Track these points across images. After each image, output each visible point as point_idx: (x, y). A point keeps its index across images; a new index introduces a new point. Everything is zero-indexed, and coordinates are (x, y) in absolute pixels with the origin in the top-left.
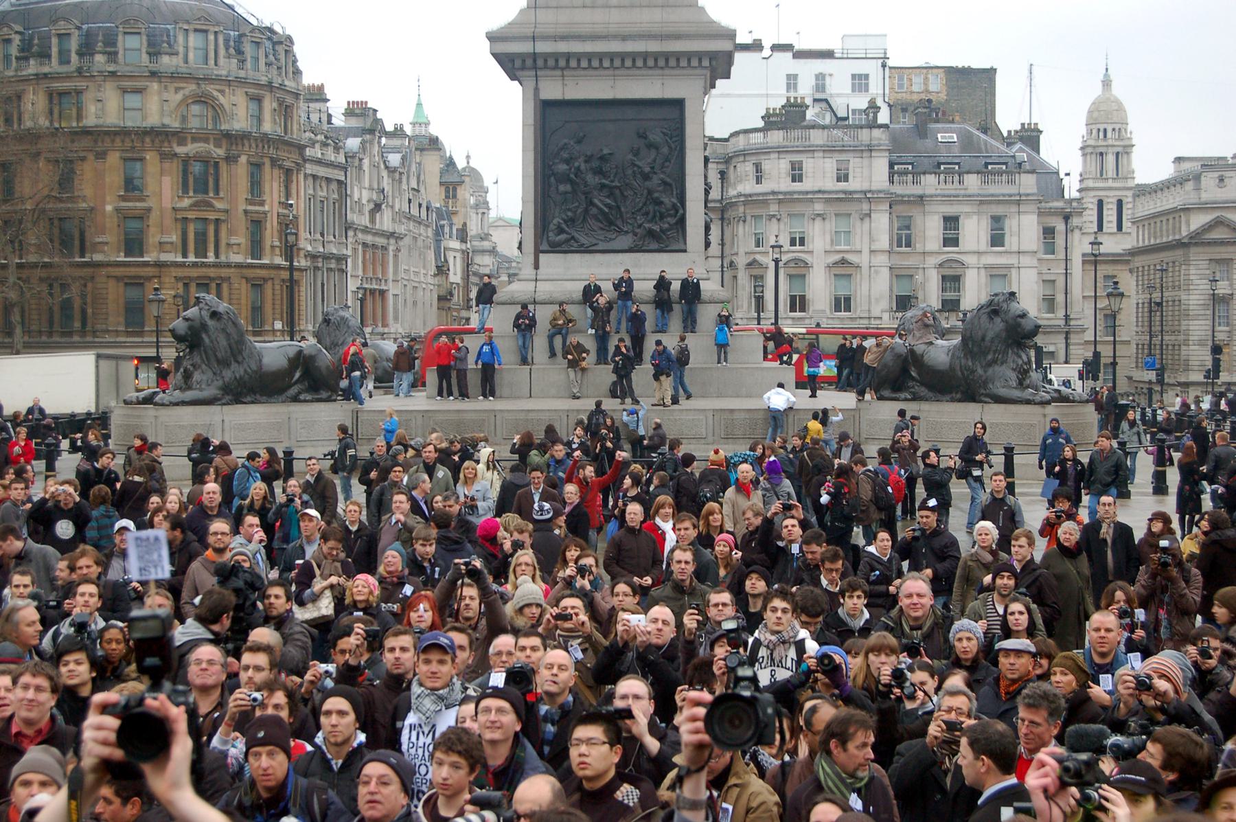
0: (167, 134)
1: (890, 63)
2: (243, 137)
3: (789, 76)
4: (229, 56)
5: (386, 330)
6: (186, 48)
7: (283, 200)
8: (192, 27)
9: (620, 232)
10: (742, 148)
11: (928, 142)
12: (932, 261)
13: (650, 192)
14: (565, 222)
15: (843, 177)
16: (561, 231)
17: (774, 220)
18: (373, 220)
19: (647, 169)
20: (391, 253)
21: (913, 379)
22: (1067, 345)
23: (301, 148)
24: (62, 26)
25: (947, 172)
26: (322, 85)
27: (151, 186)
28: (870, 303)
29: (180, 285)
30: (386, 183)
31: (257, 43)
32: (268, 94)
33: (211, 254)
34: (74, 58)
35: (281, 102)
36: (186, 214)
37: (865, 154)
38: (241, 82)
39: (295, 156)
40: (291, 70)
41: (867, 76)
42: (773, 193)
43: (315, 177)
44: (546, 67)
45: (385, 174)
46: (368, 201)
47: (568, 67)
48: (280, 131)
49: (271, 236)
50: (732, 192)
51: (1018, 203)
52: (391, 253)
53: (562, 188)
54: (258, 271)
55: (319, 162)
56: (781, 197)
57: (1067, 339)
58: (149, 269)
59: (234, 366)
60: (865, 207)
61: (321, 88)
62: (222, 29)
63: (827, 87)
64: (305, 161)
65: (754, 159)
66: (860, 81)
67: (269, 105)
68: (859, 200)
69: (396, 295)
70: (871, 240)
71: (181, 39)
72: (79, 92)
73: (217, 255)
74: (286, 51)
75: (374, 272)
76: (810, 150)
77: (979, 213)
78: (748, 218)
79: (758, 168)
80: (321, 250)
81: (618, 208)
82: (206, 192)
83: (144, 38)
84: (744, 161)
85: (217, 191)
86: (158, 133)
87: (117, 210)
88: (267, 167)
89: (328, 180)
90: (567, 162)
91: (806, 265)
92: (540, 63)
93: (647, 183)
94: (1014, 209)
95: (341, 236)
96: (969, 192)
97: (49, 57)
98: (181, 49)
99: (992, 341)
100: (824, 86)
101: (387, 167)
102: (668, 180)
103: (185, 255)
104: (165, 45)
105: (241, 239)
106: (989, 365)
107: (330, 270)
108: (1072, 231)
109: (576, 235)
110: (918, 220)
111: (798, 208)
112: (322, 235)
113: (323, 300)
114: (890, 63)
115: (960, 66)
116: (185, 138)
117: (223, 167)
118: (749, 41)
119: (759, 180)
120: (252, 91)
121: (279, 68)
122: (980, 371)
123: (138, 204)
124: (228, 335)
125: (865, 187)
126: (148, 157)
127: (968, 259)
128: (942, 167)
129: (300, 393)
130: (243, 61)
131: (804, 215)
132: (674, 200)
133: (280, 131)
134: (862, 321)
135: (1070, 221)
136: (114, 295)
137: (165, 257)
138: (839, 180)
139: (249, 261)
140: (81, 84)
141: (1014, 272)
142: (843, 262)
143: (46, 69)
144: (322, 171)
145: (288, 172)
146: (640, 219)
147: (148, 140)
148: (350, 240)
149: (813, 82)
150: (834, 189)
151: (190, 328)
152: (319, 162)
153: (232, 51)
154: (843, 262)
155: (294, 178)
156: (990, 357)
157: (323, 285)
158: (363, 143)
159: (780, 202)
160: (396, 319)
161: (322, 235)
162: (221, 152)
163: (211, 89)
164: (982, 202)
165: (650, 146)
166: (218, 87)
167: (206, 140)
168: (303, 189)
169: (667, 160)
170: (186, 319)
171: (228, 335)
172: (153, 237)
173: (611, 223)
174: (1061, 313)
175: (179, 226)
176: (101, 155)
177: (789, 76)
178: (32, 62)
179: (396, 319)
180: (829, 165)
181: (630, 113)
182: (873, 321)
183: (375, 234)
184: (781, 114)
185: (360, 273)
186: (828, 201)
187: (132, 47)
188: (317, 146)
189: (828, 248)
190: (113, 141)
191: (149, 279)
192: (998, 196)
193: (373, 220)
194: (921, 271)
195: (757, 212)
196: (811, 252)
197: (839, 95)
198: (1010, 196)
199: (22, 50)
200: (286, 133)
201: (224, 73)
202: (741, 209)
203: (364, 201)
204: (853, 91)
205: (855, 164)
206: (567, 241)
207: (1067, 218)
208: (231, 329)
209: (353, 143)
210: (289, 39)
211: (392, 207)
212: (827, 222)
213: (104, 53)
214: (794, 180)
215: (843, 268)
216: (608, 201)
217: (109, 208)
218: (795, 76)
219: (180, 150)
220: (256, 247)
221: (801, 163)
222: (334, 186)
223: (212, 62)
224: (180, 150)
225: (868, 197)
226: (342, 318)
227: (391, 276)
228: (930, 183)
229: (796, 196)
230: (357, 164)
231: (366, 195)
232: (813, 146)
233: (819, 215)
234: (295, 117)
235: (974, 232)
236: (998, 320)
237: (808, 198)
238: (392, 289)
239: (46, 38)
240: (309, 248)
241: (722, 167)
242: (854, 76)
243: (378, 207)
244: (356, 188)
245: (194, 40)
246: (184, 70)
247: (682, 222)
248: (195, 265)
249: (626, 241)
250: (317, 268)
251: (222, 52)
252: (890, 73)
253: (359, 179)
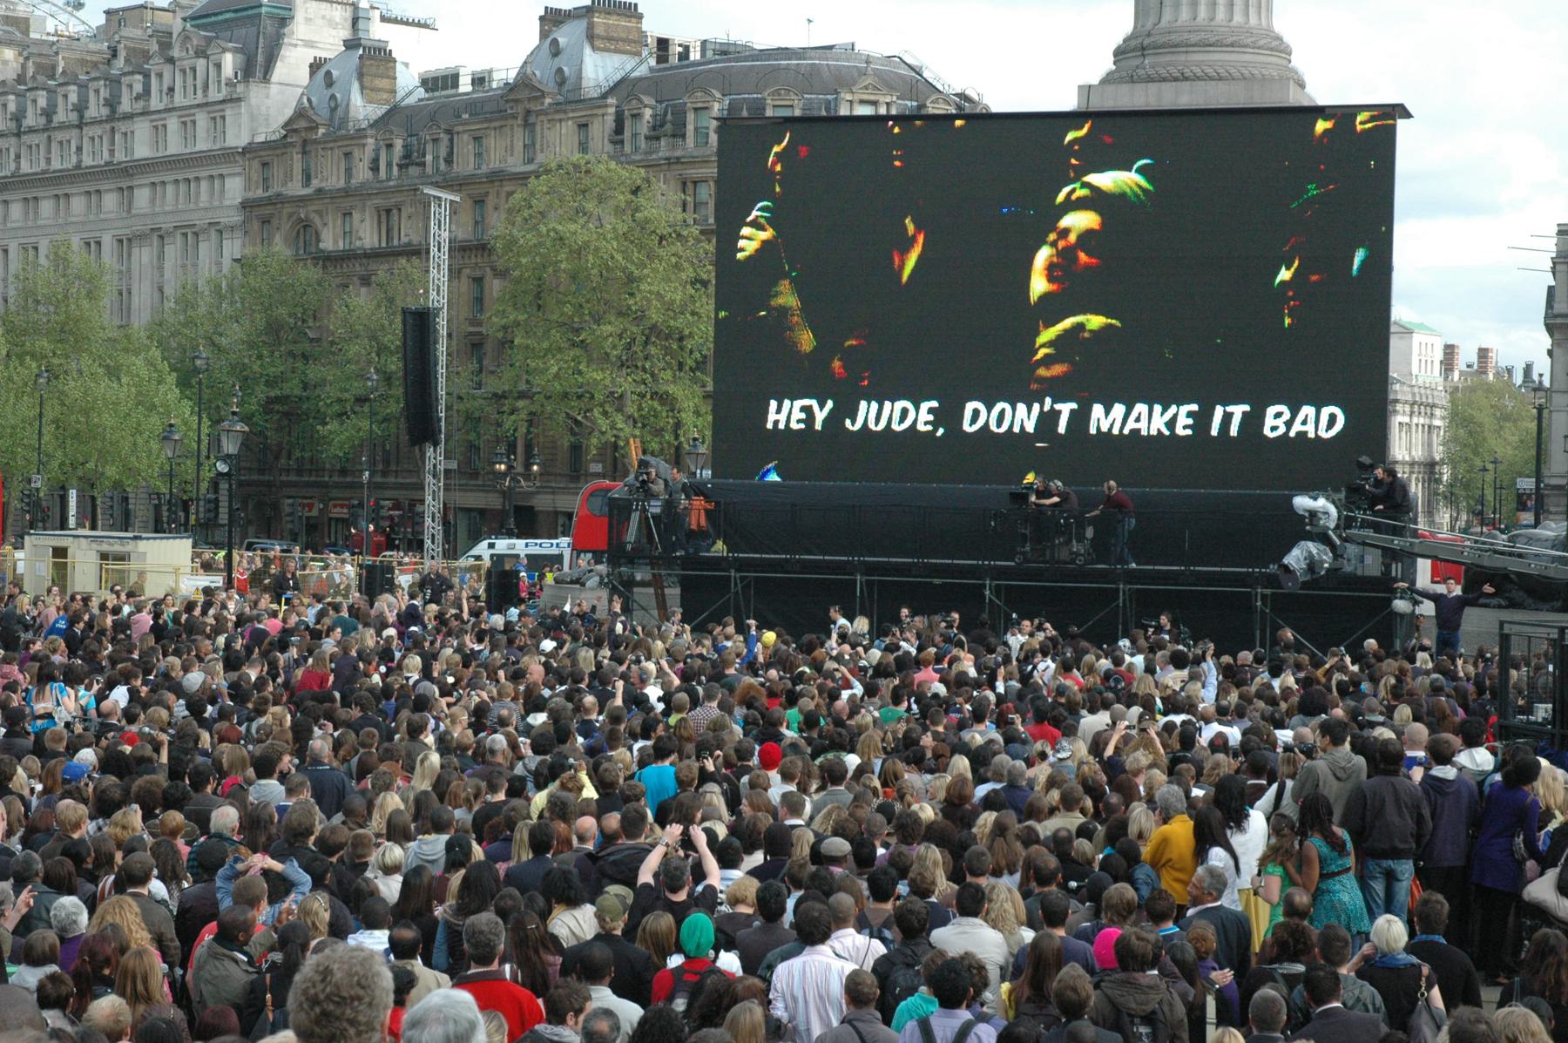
8: (857, 97)
62: (894, 99)
97: (683, 136)
143: (678, 153)
178: (663, 142)
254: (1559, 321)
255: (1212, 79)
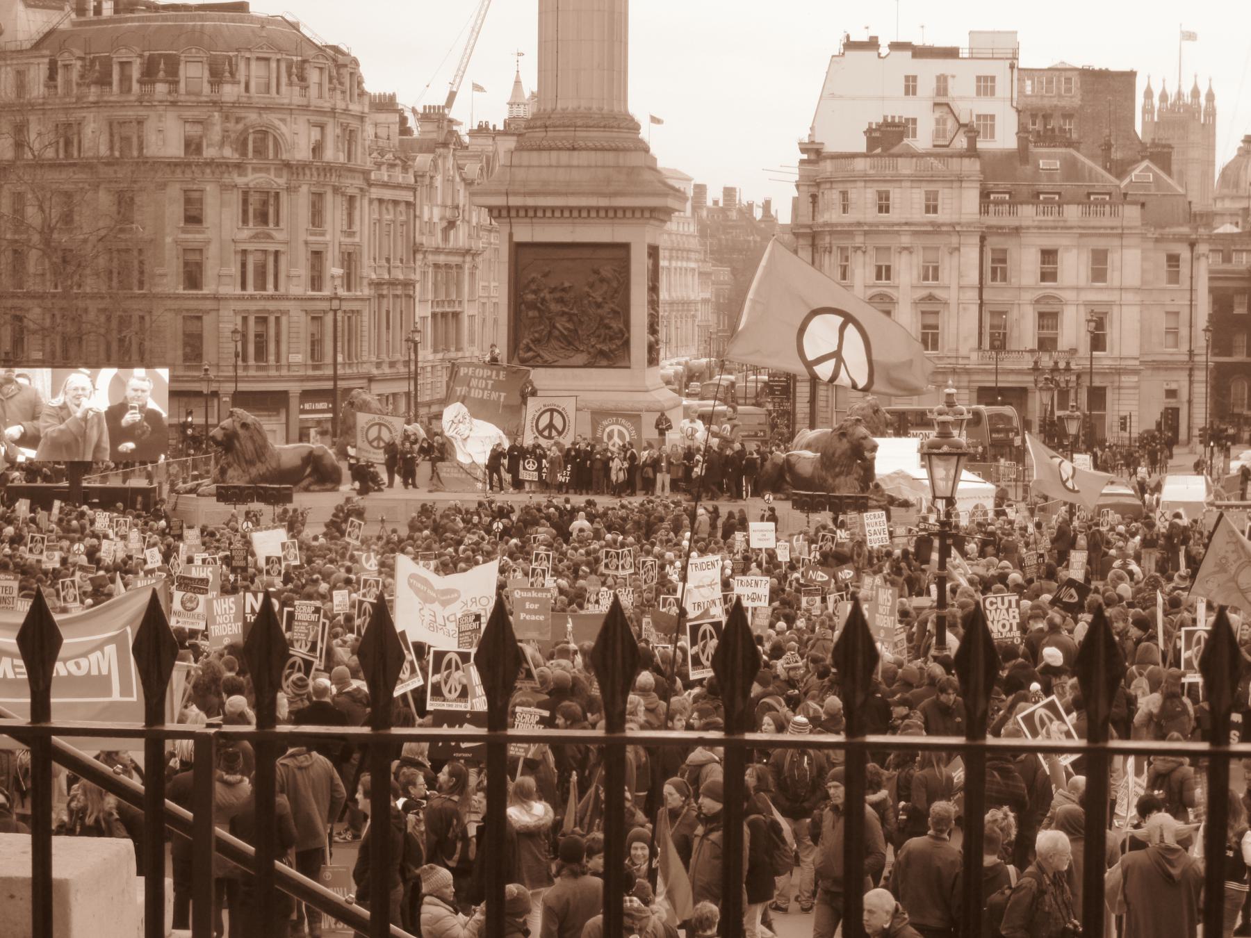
0: (227, 165)
1: (1023, 63)
2: (304, 166)
3: (907, 78)
4: (290, 84)
5: (460, 354)
6: (249, 76)
7: (345, 228)
8: (254, 55)
9: (577, 350)
10: (828, 174)
11: (1029, 169)
12: (1028, 296)
13: (602, 318)
14: (533, 341)
15: (932, 208)
16: (529, 349)
17: (859, 253)
18: (446, 238)
19: (600, 300)
20: (467, 272)
21: (788, 483)
22: (1191, 382)
23: (366, 174)
24: (123, 55)
25: (1046, 202)
26: (394, 95)
27: (211, 211)
28: (958, 340)
29: (239, 320)
30: (462, 199)
31: (321, 69)
32: (331, 120)
33: (270, 286)
34: (136, 87)
35: (345, 128)
36: (245, 247)
37: (956, 185)
38: (305, 108)
39: (359, 182)
40: (356, 91)
41: (993, 79)
42: (859, 224)
43: (381, 201)
44: (518, 216)
45: (461, 187)
46: (441, 219)
47: (535, 216)
48: (342, 158)
49: (334, 270)
50: (821, 219)
51: (1121, 236)
52: (467, 272)
53: (531, 314)
54: (318, 303)
55: (385, 185)
56: (866, 228)
57: (1190, 376)
58: (208, 302)
59: (259, 465)
60: (954, 240)
61: (392, 98)
63: (950, 90)
64: (370, 185)
65: (841, 187)
66: (986, 85)
67: (332, 131)
68: (948, 233)
69: (471, 317)
70: (960, 276)
71: (242, 66)
72: (140, 123)
73: (276, 288)
74: (351, 74)
75: (447, 294)
76: (897, 180)
77: (1078, 247)
78: (834, 248)
79: (844, 194)
80: (387, 277)
81: (576, 330)
82: (266, 222)
83: (206, 67)
84: (831, 188)
85: (277, 224)
86: (219, 165)
87: (176, 242)
88: (329, 197)
89: (396, 203)
90: (535, 292)
91: (892, 301)
92: (513, 213)
93: (599, 311)
94: (1116, 242)
95: (408, 261)
96: (1069, 224)
97: (110, 84)
98: (243, 80)
99: (840, 457)
100: (946, 89)
101: (464, 180)
102: (617, 309)
103: (244, 286)
104: (227, 74)
105: (303, 271)
106: (837, 475)
107: (396, 296)
108: (1198, 259)
109: (542, 353)
110: (1013, 256)
111: (883, 241)
112: (388, 260)
113: (388, 328)
114: (1023, 63)
115: (1097, 68)
116: (245, 169)
117: (284, 197)
118: (865, 39)
119: (845, 210)
120: (314, 118)
121: (343, 92)
122: (830, 480)
123: (198, 236)
124: (254, 442)
125: (955, 218)
126: (208, 188)
127: (1068, 295)
128: (1041, 197)
129: (310, 485)
130: (307, 87)
131: (889, 248)
132: (621, 326)
133: (342, 158)
134: (949, 361)
135: (1196, 248)
136: (170, 325)
137: (223, 290)
138: (927, 211)
139: (310, 293)
140: (142, 112)
141: (1116, 309)
142: (931, 298)
144: (388, 194)
145: (351, 199)
146: (593, 341)
147: (208, 171)
148: (419, 263)
149: (934, 84)
150: (925, 220)
151: (225, 435)
152: (385, 185)
153: (295, 78)
154: (931, 298)
155: (358, 204)
156: (837, 470)
157: (388, 312)
158: (434, 161)
159: (866, 233)
160: (472, 342)
161: (388, 260)
162: (282, 181)
163: (273, 118)
164: (1081, 235)
165: (602, 280)
166: (280, 116)
167: (267, 170)
168: (366, 213)
169: (616, 291)
170: (223, 429)
171: (254, 442)
172: (211, 270)
173: (570, 343)
174: (1185, 348)
175: (239, 257)
176: (163, 186)
177: (907, 78)
179: (472, 342)
180: (917, 196)
181: (587, 253)
182: (961, 361)
183: (450, 253)
184: (875, 130)
185: (430, 296)
186: (915, 233)
187: (193, 73)
188: (384, 168)
189: (915, 282)
190: (173, 172)
191: (208, 312)
192: (1105, 228)
193: (446, 238)
194: (1016, 307)
195: (843, 243)
196: (897, 287)
197: (962, 98)
198: (1112, 228)
199: (82, 77)
200: (349, 159)
201: (286, 101)
202: (827, 239)
203: (436, 219)
204: (978, 93)
205: (946, 196)
206: (534, 358)
207: (1192, 245)
208: (257, 437)
209: (422, 160)
210: (355, 62)
211: (469, 222)
212: (914, 256)
213: (167, 82)
214: (880, 210)
215: (930, 307)
216: (568, 325)
217: (169, 240)
218: (915, 78)
219: (240, 181)
220: (316, 281)
221: (887, 192)
222: (402, 208)
223: (274, 89)
224: (240, 181)
225: (955, 229)
226: (364, 401)
227: (466, 296)
228: (1027, 213)
229: (882, 228)
230: (427, 181)
231: (437, 212)
232: (900, 175)
233: (905, 248)
234: (360, 141)
235: (1073, 266)
236: (845, 440)
237: (893, 230)
238: (468, 310)
239: (107, 65)
240: (374, 276)
241: (813, 190)
242: (979, 79)
243: (451, 224)
244: (426, 209)
245: (257, 70)
246: (244, 100)
247: (627, 343)
248: (252, 298)
249: (581, 358)
250: (381, 296)
251: (284, 79)
252: (1019, 74)
253: (430, 198)
254: (802, 230)
255: (592, 149)
